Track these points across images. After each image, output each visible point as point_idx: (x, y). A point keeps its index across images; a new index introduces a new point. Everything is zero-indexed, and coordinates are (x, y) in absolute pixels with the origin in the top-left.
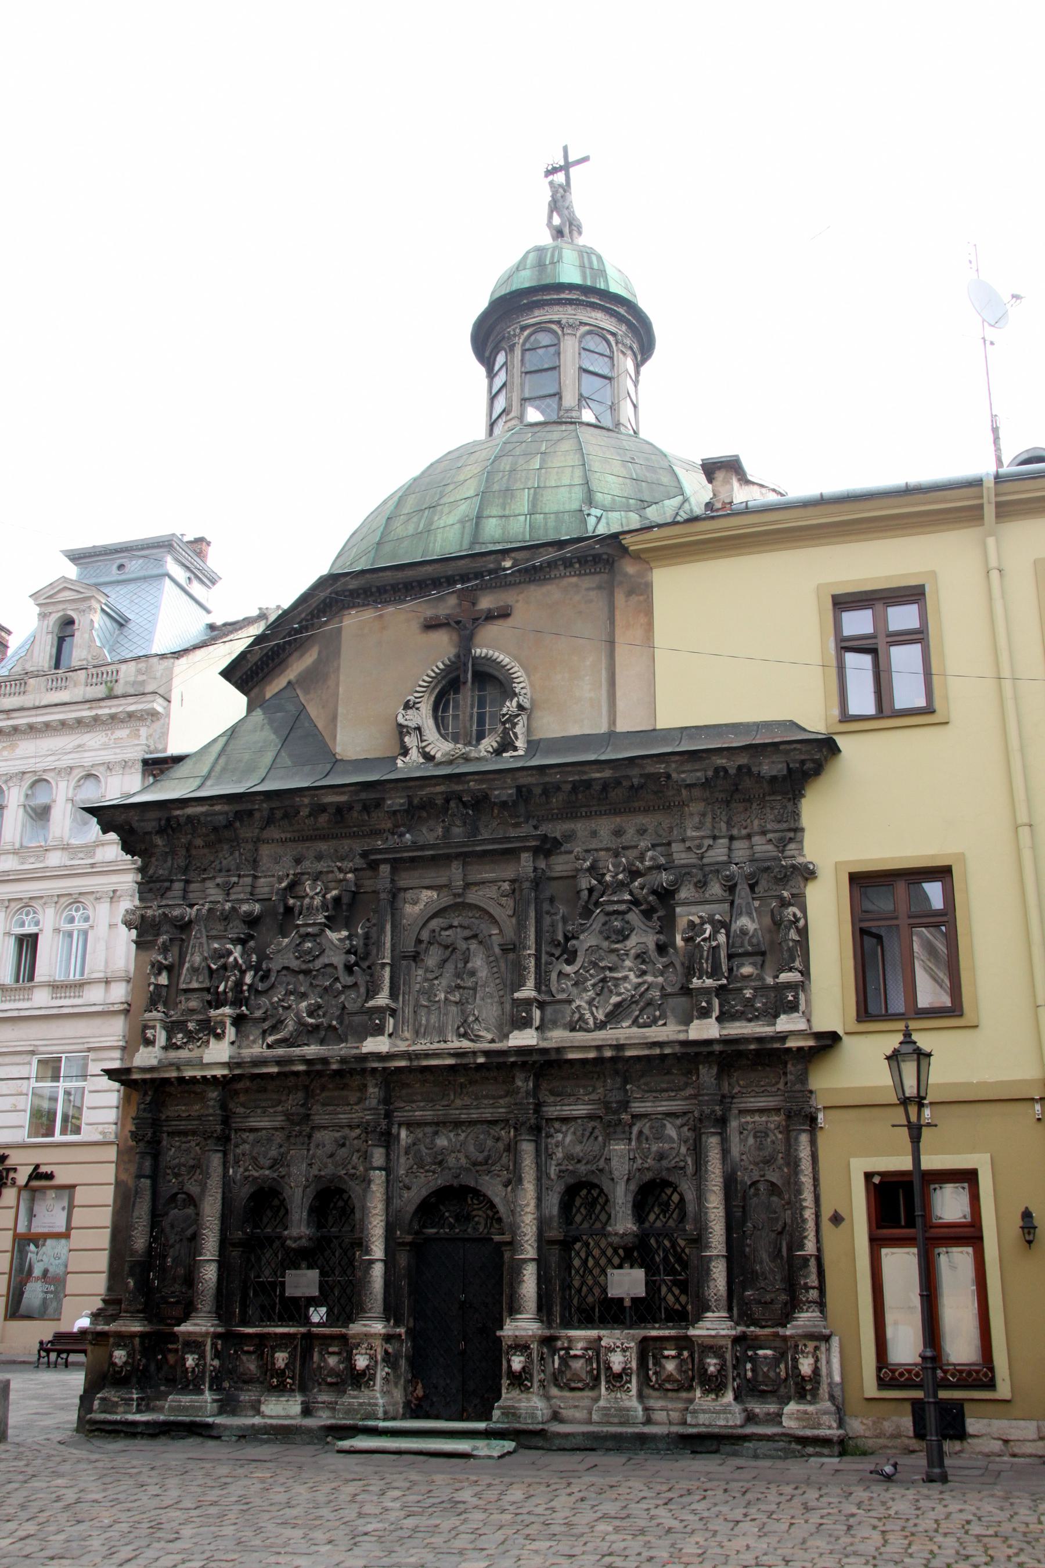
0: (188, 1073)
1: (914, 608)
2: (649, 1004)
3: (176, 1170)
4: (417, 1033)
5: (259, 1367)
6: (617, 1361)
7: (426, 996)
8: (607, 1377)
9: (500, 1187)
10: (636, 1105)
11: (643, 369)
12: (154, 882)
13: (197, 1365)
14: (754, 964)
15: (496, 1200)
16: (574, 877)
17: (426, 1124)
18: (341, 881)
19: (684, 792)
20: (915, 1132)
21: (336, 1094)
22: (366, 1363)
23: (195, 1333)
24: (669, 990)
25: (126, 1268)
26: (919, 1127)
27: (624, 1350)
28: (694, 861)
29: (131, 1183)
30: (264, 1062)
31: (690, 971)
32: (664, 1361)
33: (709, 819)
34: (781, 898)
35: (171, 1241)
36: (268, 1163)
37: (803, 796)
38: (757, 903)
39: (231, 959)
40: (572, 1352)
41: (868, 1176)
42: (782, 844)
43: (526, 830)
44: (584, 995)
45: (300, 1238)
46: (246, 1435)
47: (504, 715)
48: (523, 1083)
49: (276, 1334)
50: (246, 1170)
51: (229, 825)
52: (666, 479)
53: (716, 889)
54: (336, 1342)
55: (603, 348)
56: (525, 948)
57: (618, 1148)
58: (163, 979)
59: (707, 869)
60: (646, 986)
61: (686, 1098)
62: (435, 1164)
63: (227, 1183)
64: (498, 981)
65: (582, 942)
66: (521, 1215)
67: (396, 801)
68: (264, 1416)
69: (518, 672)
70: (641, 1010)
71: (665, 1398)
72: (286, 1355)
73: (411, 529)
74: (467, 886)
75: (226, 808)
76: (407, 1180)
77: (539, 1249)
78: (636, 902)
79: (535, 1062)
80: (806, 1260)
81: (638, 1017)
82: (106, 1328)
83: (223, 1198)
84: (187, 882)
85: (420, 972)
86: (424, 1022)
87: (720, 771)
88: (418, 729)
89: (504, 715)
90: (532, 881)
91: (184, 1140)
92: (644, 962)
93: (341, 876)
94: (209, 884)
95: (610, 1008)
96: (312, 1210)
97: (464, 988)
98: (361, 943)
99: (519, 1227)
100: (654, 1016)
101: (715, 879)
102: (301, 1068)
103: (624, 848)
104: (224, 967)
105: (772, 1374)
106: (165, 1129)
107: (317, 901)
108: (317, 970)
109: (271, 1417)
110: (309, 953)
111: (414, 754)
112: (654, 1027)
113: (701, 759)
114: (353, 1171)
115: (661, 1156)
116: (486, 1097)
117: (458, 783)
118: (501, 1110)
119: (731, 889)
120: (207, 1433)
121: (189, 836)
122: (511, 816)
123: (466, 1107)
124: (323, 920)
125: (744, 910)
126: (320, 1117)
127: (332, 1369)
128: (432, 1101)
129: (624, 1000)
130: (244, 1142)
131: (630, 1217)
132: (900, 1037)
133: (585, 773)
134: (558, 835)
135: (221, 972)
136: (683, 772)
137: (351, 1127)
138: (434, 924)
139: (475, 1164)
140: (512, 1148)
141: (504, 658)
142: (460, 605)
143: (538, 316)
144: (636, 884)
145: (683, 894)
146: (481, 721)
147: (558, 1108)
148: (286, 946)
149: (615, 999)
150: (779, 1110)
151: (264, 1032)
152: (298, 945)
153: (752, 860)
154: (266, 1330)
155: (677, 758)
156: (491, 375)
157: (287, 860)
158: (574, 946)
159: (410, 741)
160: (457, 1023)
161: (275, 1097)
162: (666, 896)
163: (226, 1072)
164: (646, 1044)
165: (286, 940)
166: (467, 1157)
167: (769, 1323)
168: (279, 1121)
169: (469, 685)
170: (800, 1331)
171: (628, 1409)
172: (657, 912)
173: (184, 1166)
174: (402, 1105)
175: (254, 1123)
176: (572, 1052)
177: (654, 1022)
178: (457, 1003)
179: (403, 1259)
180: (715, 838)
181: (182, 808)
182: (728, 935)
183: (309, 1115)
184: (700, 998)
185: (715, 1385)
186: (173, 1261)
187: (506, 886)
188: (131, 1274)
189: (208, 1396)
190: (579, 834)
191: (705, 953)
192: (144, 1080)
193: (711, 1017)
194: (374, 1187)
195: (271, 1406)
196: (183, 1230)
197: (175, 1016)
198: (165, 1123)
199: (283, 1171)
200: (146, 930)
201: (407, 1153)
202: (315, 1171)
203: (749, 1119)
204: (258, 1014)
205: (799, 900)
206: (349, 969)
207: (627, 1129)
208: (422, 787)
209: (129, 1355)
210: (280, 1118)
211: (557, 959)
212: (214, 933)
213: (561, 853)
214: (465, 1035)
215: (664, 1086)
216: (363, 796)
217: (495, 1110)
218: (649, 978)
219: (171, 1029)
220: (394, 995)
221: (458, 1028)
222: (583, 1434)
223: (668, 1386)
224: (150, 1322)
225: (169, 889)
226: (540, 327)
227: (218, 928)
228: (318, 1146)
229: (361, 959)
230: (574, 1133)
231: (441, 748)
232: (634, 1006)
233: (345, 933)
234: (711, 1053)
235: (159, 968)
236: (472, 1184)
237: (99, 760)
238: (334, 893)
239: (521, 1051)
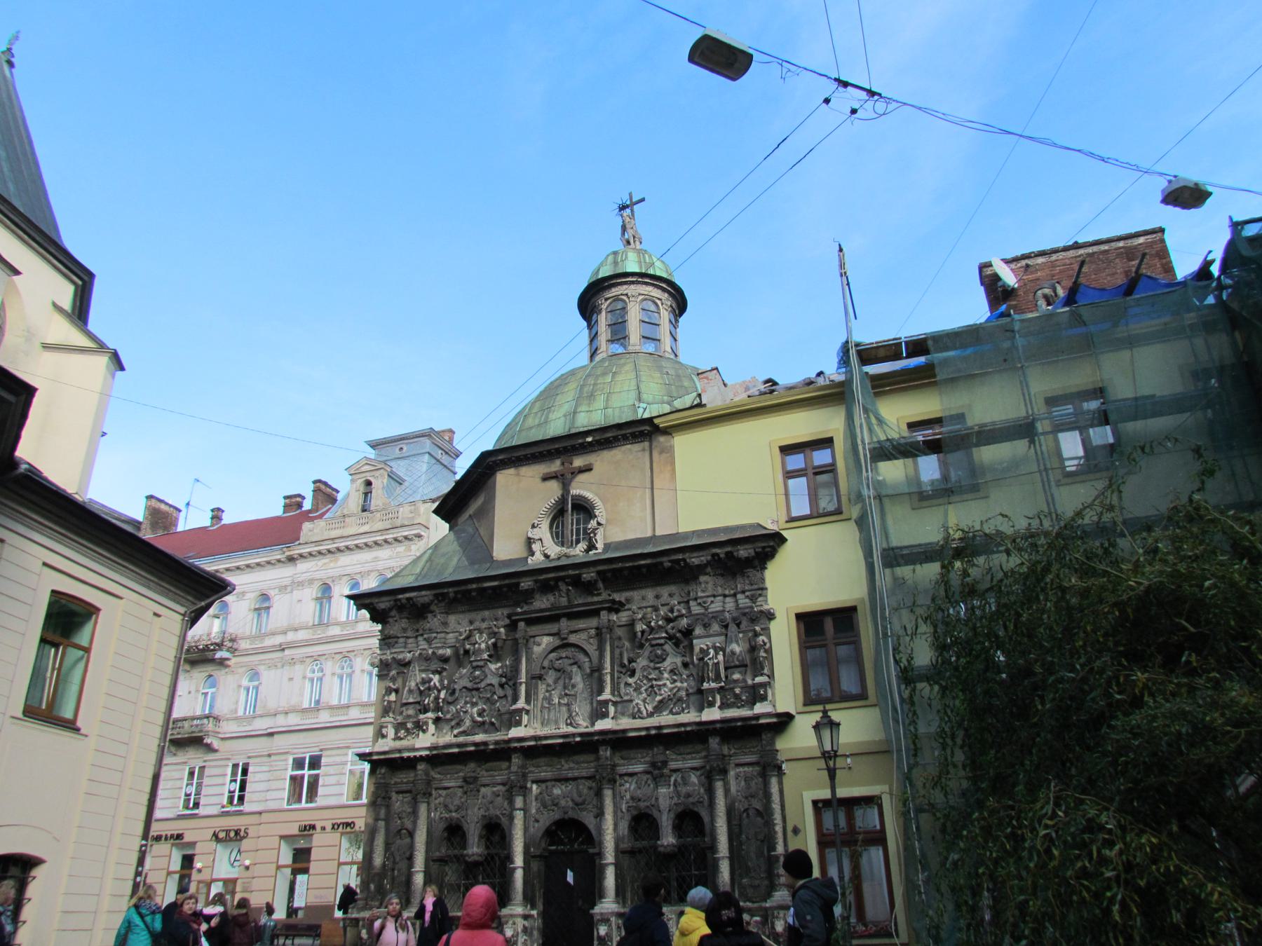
0: (406, 755)
1: (828, 451)
11: (681, 320)
20: (832, 773)
26: (835, 769)
28: (703, 611)
31: (702, 680)
33: (710, 586)
34: (755, 631)
41: (815, 803)
42: (753, 599)
43: (604, 596)
48: (605, 752)
52: (686, 384)
53: (716, 627)
55: (653, 308)
57: (663, 790)
69: (598, 503)
73: (537, 422)
74: (572, 632)
77: (616, 857)
78: (670, 638)
80: (777, 857)
83: (428, 832)
94: (420, 638)
96: (481, 837)
102: (472, 748)
104: (429, 689)
107: (483, 646)
115: (688, 795)
123: (570, 769)
132: (821, 714)
134: (623, 600)
139: (577, 804)
140: (599, 794)
141: (589, 495)
142: (563, 464)
143: (615, 291)
146: (578, 534)
149: (659, 698)
150: (756, 763)
153: (737, 607)
156: (590, 327)
157: (465, 622)
159: (536, 547)
160: (566, 716)
169: (572, 513)
177: (683, 710)
179: (535, 866)
180: (714, 596)
194: (516, 821)
197: (400, 719)
199: (463, 813)
200: (384, 669)
202: (482, 812)
203: (741, 769)
204: (448, 716)
205: (766, 631)
206: (502, 686)
214: (571, 724)
216: (507, 582)
218: (679, 684)
219: (399, 726)
220: (528, 701)
226: (617, 299)
229: (510, 680)
231: (554, 550)
234: (715, 729)
235: (389, 691)
237: (387, 566)
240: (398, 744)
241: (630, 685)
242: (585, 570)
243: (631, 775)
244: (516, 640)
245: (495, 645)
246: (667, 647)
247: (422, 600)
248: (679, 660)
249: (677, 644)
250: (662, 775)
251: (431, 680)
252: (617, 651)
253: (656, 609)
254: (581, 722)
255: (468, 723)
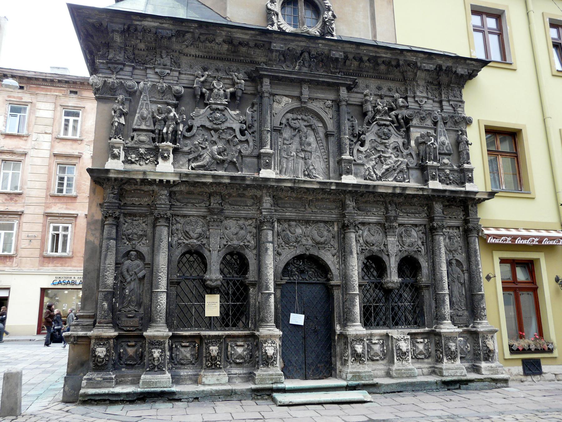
0: (150, 177)
2: (401, 171)
3: (130, 237)
4: (281, 172)
5: (192, 355)
6: (404, 346)
7: (286, 153)
8: (397, 354)
9: (331, 256)
10: (400, 219)
12: (112, 63)
13: (161, 356)
14: (448, 159)
15: (329, 263)
16: (361, 106)
17: (290, 220)
18: (237, 83)
19: (419, 73)
21: (239, 199)
22: (273, 351)
23: (158, 336)
24: (411, 165)
25: (101, 296)
27: (405, 340)
29: (97, 242)
30: (204, 176)
32: (417, 344)
35: (129, 280)
36: (195, 236)
37: (463, 87)
38: (446, 132)
39: (172, 114)
40: (374, 342)
44: (371, 162)
45: (216, 280)
46: (196, 398)
47: (326, 18)
49: (209, 336)
50: (180, 239)
51: (170, 38)
53: (429, 122)
54: (241, 340)
56: (345, 134)
58: (122, 120)
59: (428, 112)
60: (400, 162)
61: (423, 218)
62: (296, 242)
63: (170, 245)
64: (323, 151)
65: (367, 137)
66: (353, 271)
67: (277, 46)
68: (204, 385)
70: (398, 174)
71: (418, 362)
72: (216, 348)
75: (171, 27)
76: (280, 251)
79: (361, 192)
81: (396, 177)
82: (89, 333)
84: (134, 68)
85: (280, 140)
86: (285, 166)
87: (440, 67)
88: (277, 15)
89: (326, 18)
90: (347, 102)
91: (135, 219)
92: (397, 151)
93: (238, 81)
94: (149, 71)
95: (383, 171)
97: (306, 151)
98: (250, 118)
99: (352, 277)
100: (404, 177)
102: (227, 181)
103: (386, 96)
105: (464, 349)
106: (122, 211)
107: (222, 92)
108: (223, 130)
109: (209, 385)
110: (219, 119)
111: (276, 24)
112: (403, 183)
113: (432, 59)
114: (247, 243)
115: (412, 245)
116: (325, 208)
117: (313, 43)
118: (333, 216)
119: (435, 123)
120: (171, 398)
121: (138, 41)
122: (333, 68)
124: (227, 103)
126: (229, 211)
127: (240, 355)
128: (295, 208)
129: (390, 168)
130: (178, 222)
131: (397, 274)
133: (378, 53)
135: (163, 122)
136: (424, 63)
137: (246, 219)
138: (290, 116)
139: (318, 243)
144: (393, 113)
147: (363, 217)
148: (203, 114)
149: (385, 167)
150: (458, 227)
151: (189, 160)
152: (211, 114)
154: (203, 333)
155: (422, 55)
158: (364, 138)
161: (201, 198)
162: (407, 120)
163: (177, 179)
164: (417, 188)
165: (202, 111)
166: (313, 239)
167: (462, 325)
168: (203, 211)
170: (486, 329)
171: (410, 370)
172: (402, 128)
173: (136, 234)
174: (279, 208)
175: (185, 211)
176: (381, 188)
178: (302, 158)
180: (428, 98)
181: (141, 21)
183: (223, 209)
185: (452, 356)
186: (130, 292)
187: (330, 102)
188: (107, 300)
189: (168, 375)
190: (361, 85)
192: (116, 179)
195: (209, 378)
196: (136, 274)
198: (122, 208)
201: (278, 235)
204: (186, 149)
205: (464, 133)
206: (242, 132)
207: (395, 230)
208: (293, 41)
209: (108, 351)
210: (203, 210)
211: (355, 143)
212: (154, 100)
213: (353, 92)
214: (308, 175)
215: (413, 211)
217: (330, 216)
219: (128, 150)
221: (304, 171)
222: (396, 384)
223: (421, 357)
224: (116, 331)
225: (122, 69)
227: (157, 98)
228: (226, 229)
230: (369, 231)
232: (393, 171)
233: (238, 112)
234: (444, 197)
235: (122, 114)
236: (316, 254)
238: (232, 89)
239: (354, 185)
240: (129, 167)
241: (361, 152)
242: (333, 48)
243: (363, 224)
244: (259, 95)
245: (233, 95)
246: (390, 128)
247: (164, 33)
248: (400, 141)
249: (398, 128)
250: (391, 227)
251: (171, 111)
252: (350, 123)
253: (381, 97)
254: (317, 176)
255: (206, 159)
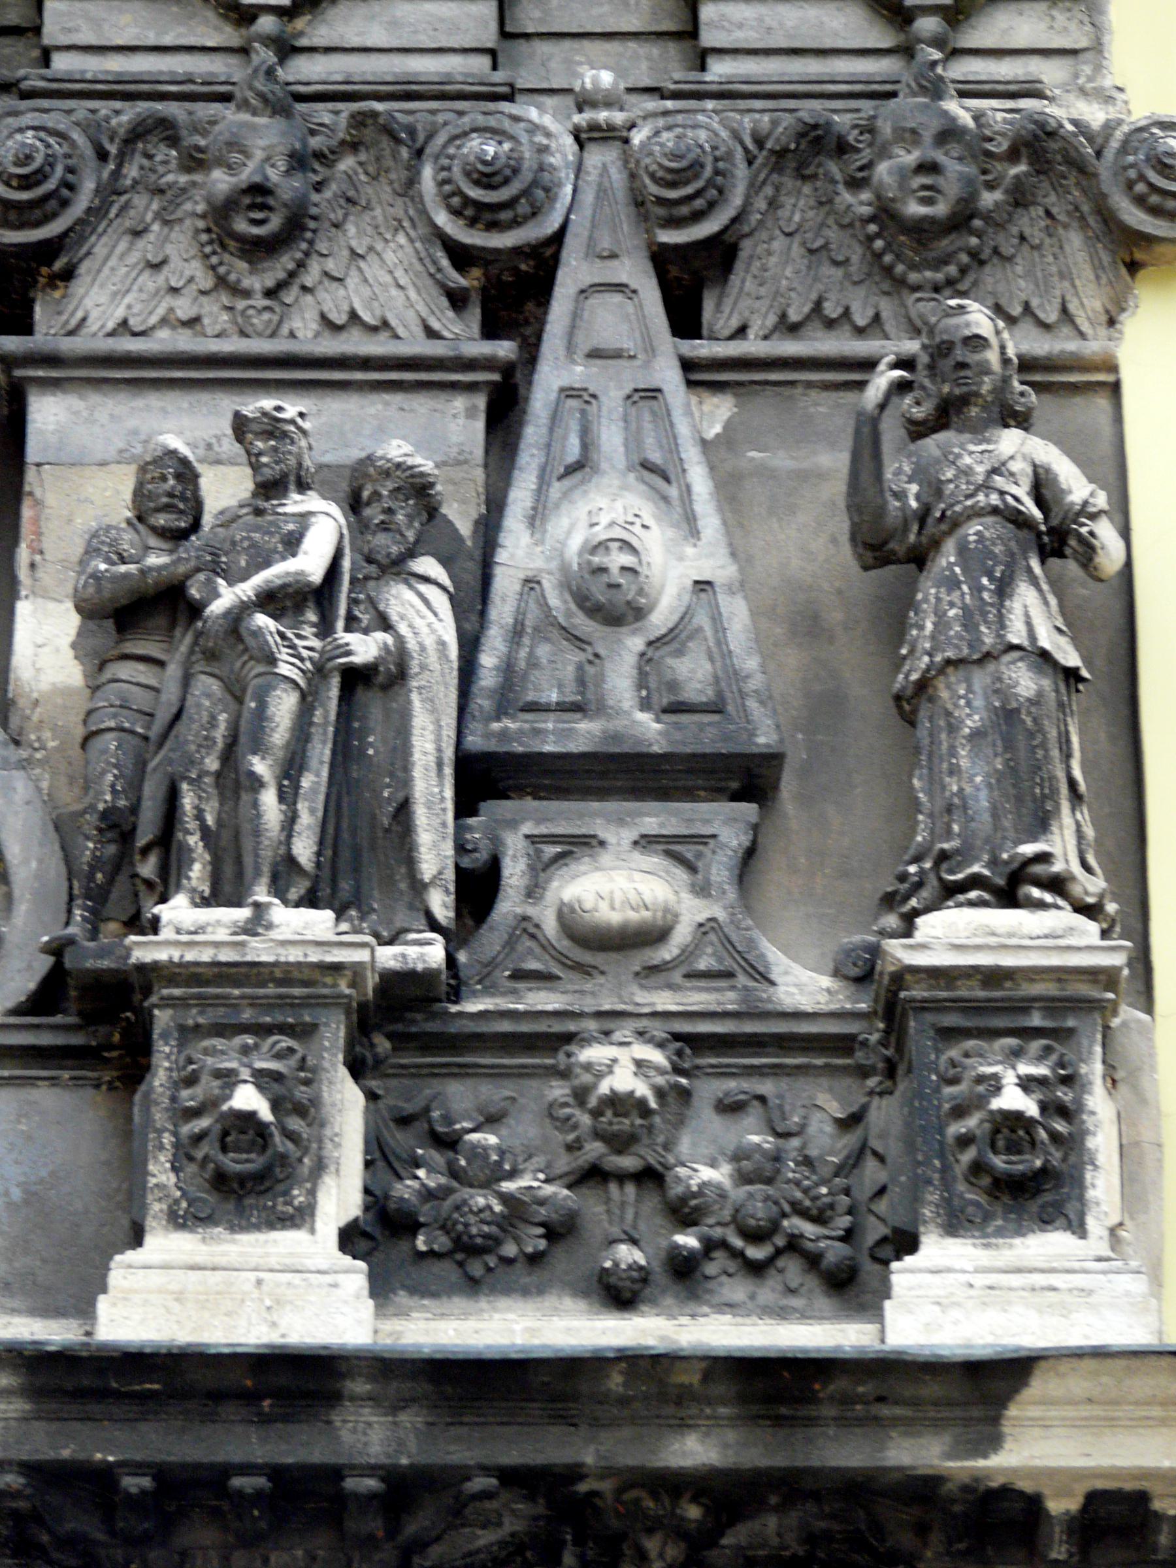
14: (678, 850)
53: (382, 280)
101: (382, 200)
125: (611, 439)
145: (107, 297)
182: (472, 602)
184: (225, 1054)
191: (283, 707)
193: (300, 1217)
234: (309, 1496)
